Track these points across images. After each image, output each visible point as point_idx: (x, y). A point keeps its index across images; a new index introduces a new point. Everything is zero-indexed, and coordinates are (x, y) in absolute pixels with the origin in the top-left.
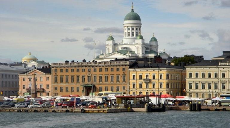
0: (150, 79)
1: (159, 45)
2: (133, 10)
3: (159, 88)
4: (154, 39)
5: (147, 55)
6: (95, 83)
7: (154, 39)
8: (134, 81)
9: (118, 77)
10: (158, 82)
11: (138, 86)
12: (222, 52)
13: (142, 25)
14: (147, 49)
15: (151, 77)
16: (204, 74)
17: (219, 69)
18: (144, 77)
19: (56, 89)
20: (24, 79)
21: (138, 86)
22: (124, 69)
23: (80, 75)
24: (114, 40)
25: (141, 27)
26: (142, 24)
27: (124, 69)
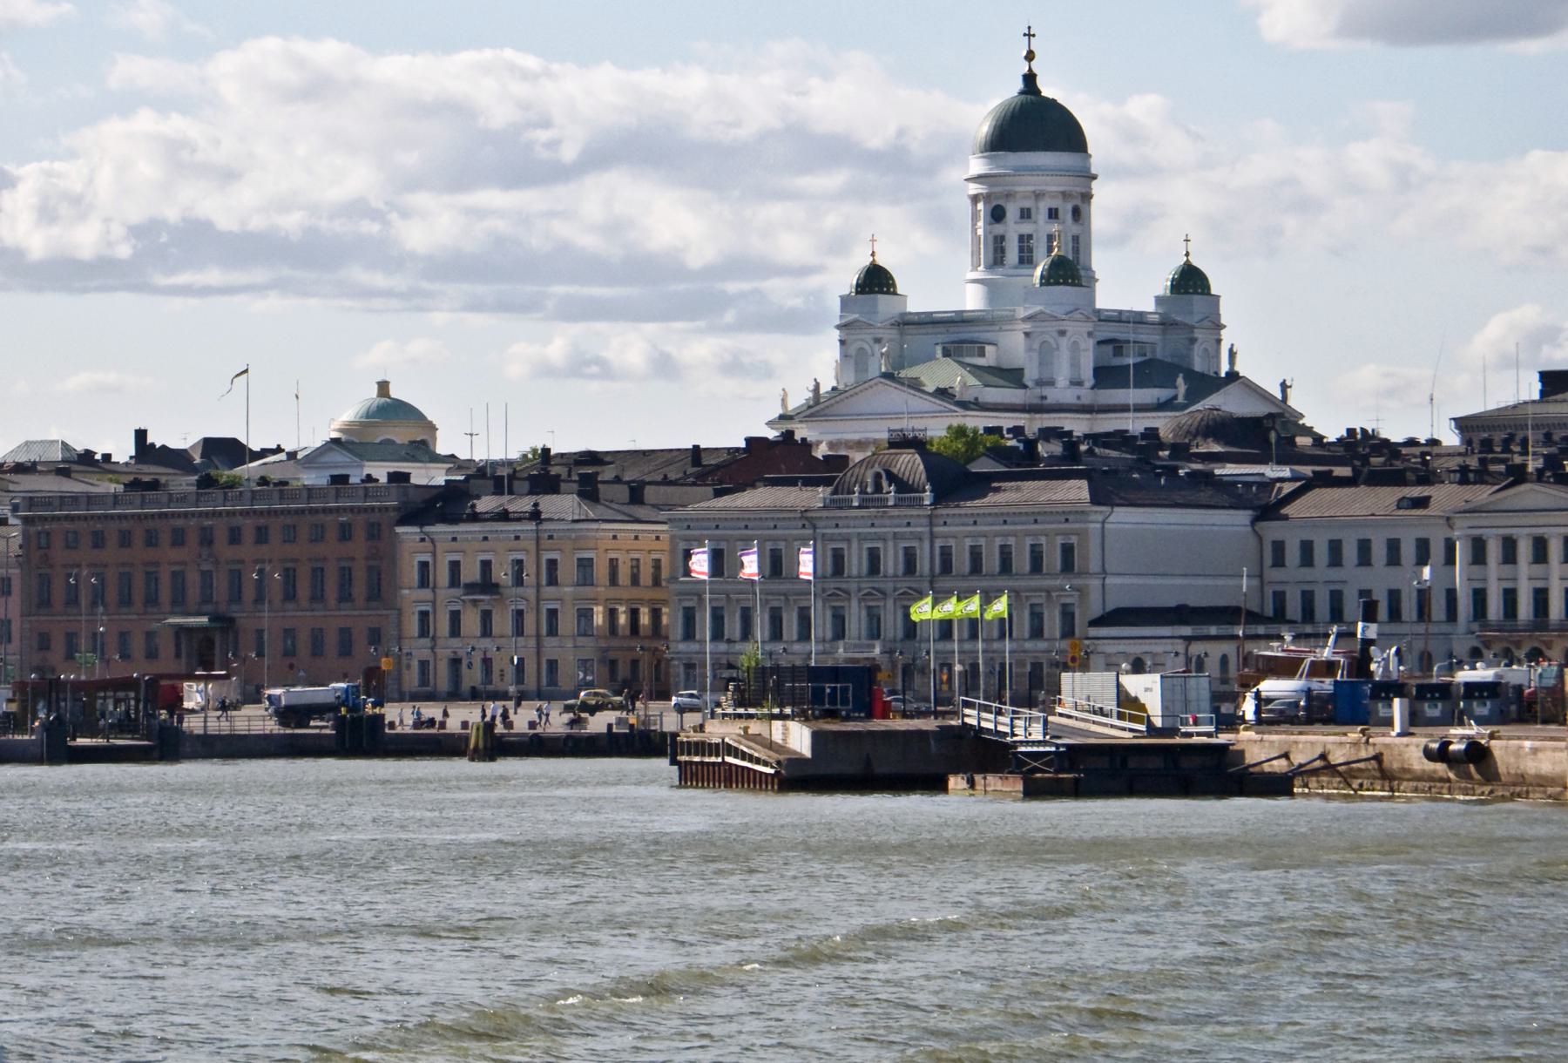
0: (497, 586)
1: (1223, 321)
2: (1030, 79)
3: (544, 631)
4: (1190, 281)
5: (1102, 391)
6: (234, 607)
7: (1190, 281)
8: (426, 594)
9: (346, 577)
10: (538, 600)
11: (443, 625)
12: (1537, 377)
13: (1094, 184)
14: (1117, 346)
15: (502, 575)
16: (1007, 550)
17: (815, 527)
18: (471, 573)
19: (44, 643)
20: (291, 572)
21: (443, 625)
22: (374, 532)
23: (106, 566)
24: (895, 293)
25: (1087, 197)
26: (1094, 177)
27: (374, 532)
